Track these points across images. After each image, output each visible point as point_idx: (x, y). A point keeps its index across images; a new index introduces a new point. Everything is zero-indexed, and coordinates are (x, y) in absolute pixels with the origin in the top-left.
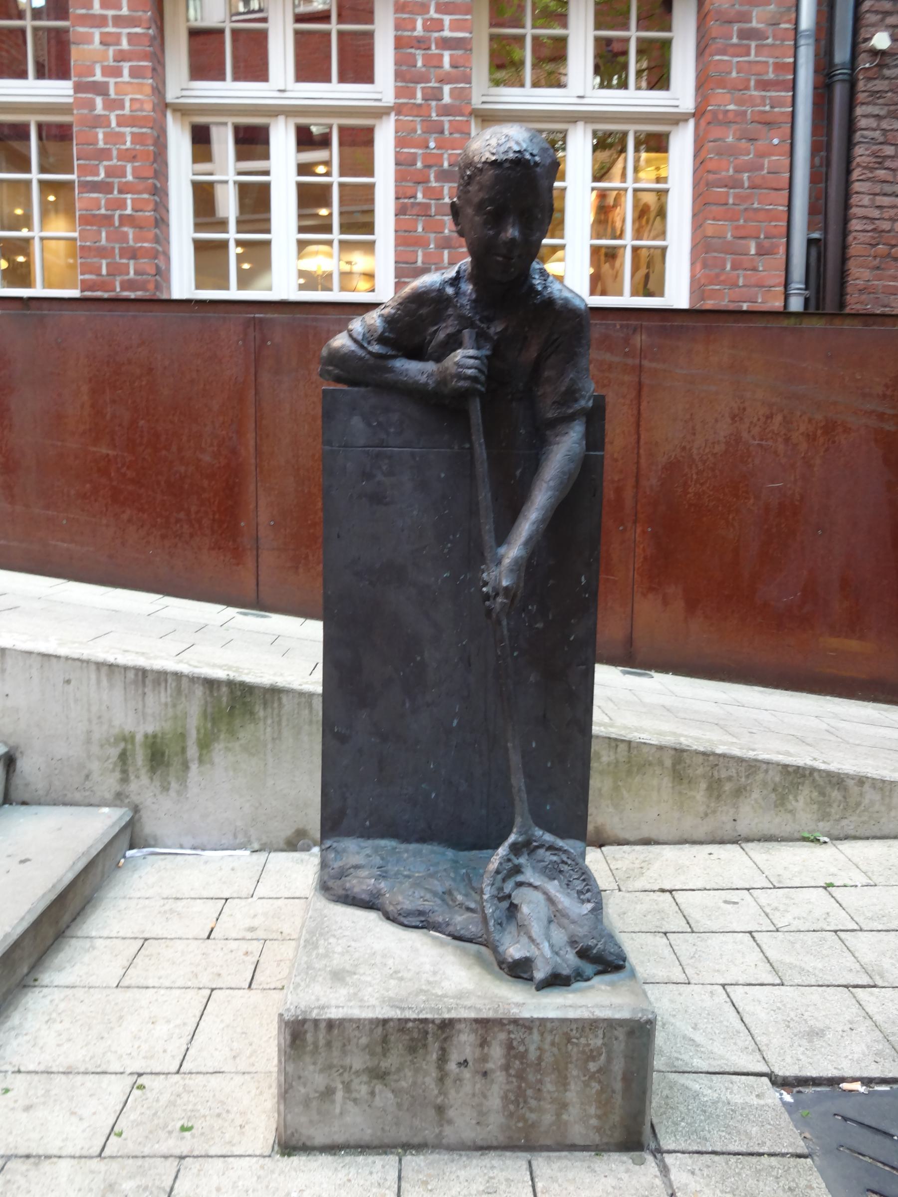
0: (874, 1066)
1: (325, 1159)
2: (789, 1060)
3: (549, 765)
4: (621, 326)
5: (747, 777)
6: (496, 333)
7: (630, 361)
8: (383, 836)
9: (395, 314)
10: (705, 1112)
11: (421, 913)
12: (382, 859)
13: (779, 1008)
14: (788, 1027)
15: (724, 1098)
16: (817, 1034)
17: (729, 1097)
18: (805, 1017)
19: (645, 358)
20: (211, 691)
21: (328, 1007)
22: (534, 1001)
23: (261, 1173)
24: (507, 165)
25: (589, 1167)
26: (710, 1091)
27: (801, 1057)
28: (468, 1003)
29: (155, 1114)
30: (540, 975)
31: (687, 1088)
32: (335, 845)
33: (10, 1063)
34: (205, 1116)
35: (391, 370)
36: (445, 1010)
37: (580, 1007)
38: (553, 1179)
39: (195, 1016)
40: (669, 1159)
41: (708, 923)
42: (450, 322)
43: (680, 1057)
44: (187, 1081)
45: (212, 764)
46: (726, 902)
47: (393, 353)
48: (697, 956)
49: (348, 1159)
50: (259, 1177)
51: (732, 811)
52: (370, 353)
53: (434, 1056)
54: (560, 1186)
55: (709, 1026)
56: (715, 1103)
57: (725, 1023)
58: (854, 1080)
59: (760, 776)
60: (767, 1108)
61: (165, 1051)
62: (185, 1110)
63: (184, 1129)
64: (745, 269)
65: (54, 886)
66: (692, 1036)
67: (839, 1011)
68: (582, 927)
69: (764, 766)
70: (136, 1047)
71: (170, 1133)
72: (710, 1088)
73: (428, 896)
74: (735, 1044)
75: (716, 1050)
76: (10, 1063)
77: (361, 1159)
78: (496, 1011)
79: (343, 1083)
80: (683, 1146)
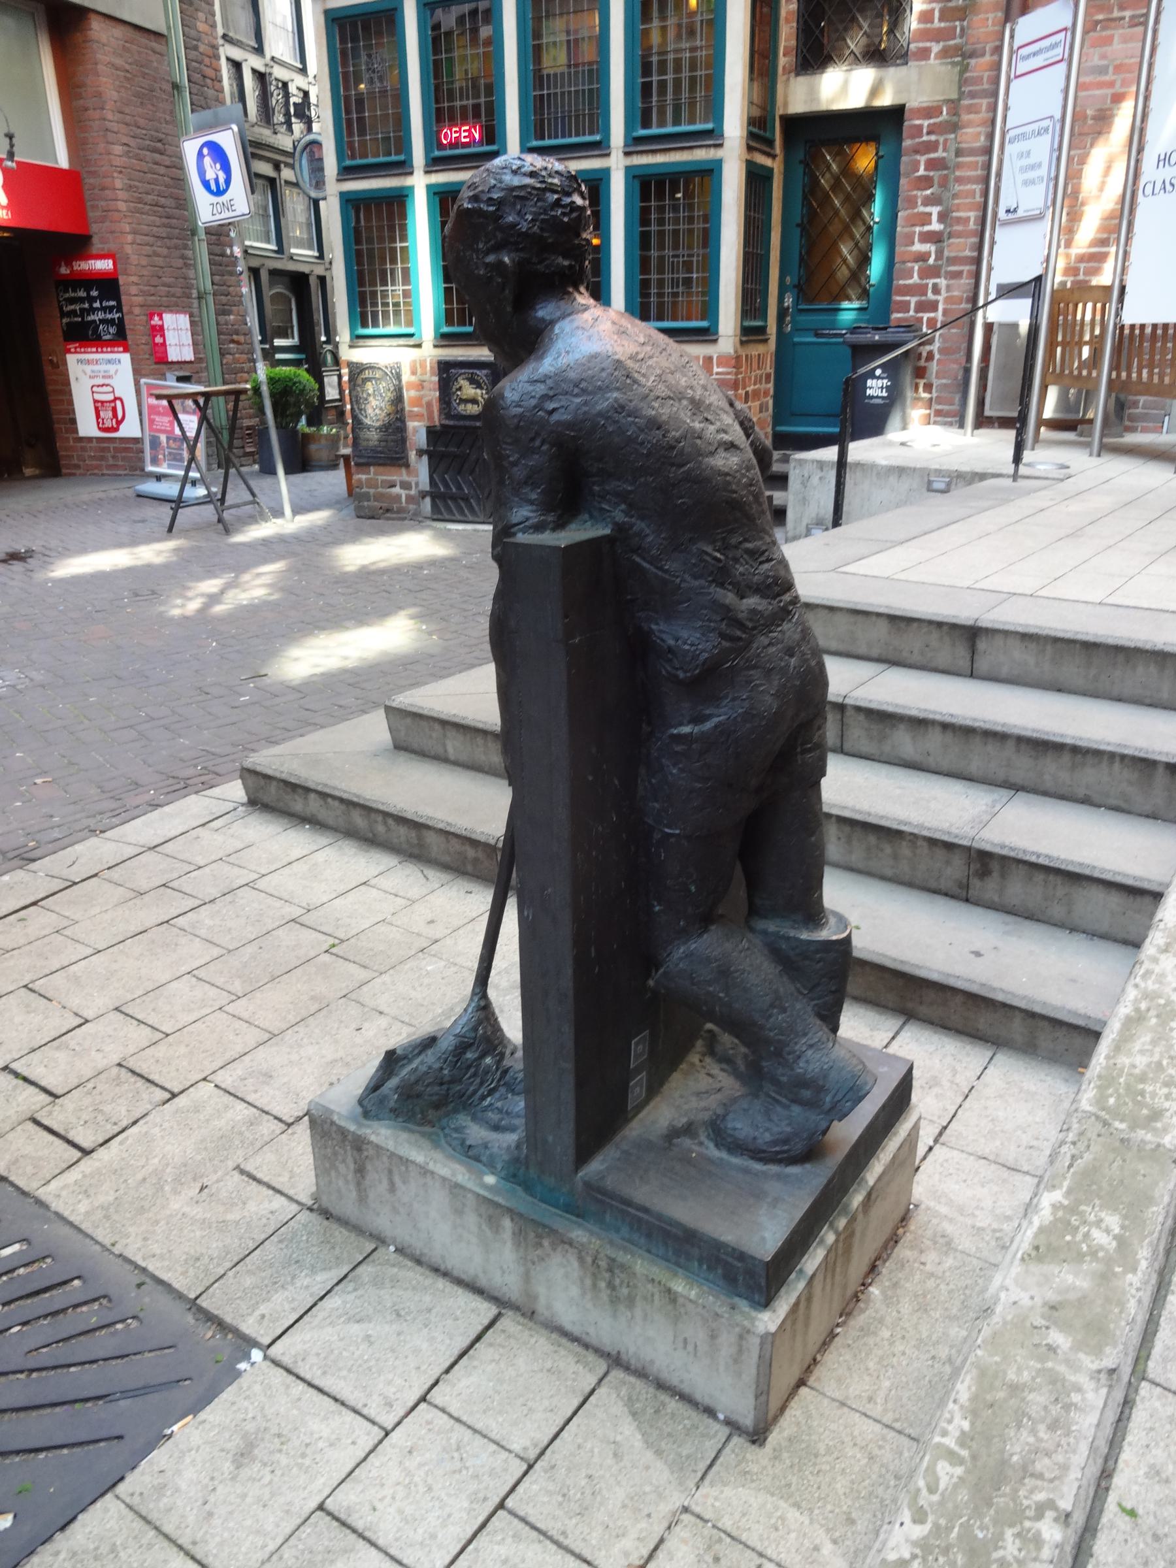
2: (257, 1388)
10: (297, 1262)
13: (303, 1456)
14: (279, 1436)
15: (290, 1288)
16: (242, 1455)
17: (286, 1293)
18: (269, 1469)
26: (305, 1283)
27: (246, 1403)
31: (325, 1269)
40: (294, 1208)
41: (503, 1551)
43: (355, 1294)
48: (456, 1455)
55: (358, 1353)
56: (294, 1277)
57: (344, 1373)
65: (902, 962)
66: (364, 1326)
67: (231, 1525)
72: (307, 1287)
74: (318, 1354)
75: (330, 1330)
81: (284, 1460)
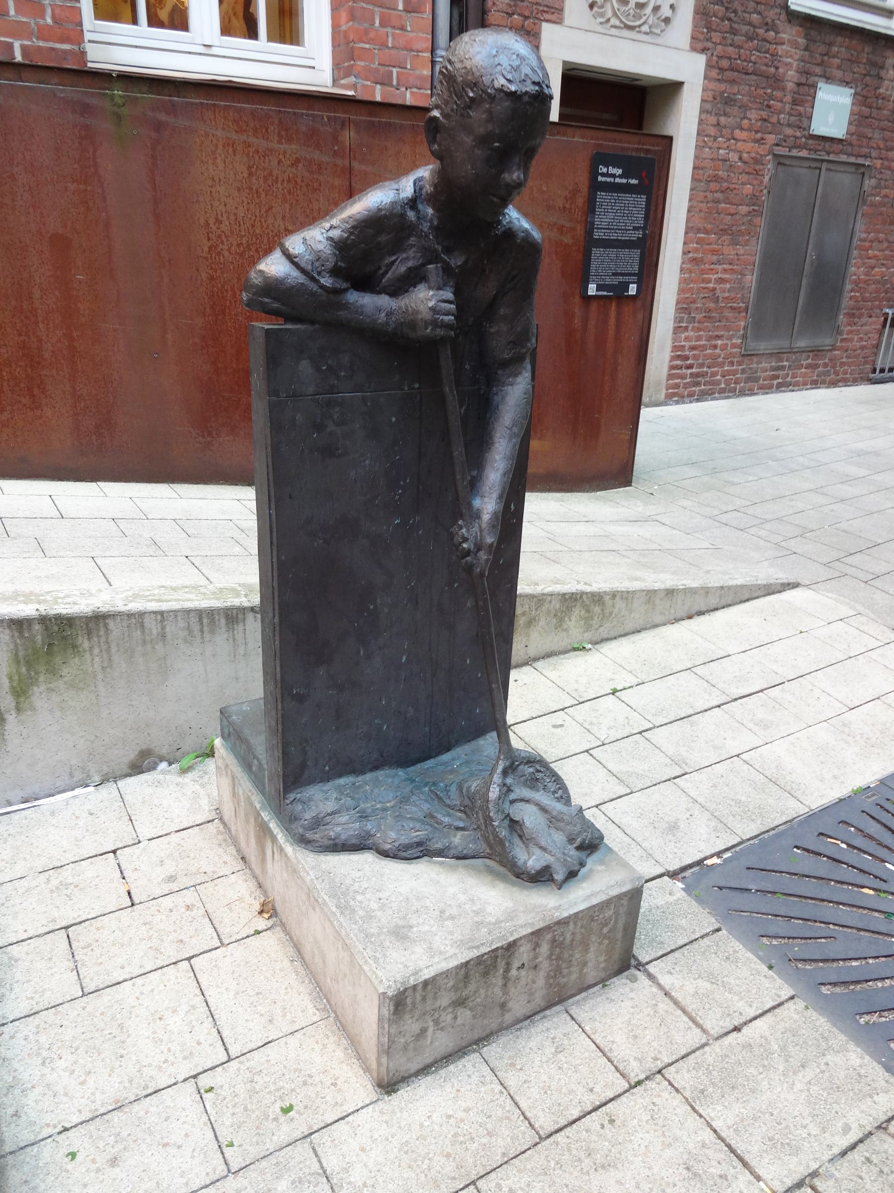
0: (718, 841)
1: (425, 1082)
2: (670, 856)
3: (479, 675)
4: (329, 118)
5: (536, 610)
6: (457, 267)
7: (339, 162)
8: (340, 776)
9: (347, 238)
11: (419, 844)
12: (353, 798)
19: (355, 159)
20: (21, 633)
21: (420, 970)
22: (565, 900)
23: (385, 1118)
24: (526, 98)
25: (607, 999)
27: (676, 850)
28: (521, 922)
29: (246, 1109)
30: (559, 877)
32: (299, 796)
33: (48, 1125)
34: (293, 1090)
35: (346, 306)
36: (508, 935)
37: (598, 892)
38: (593, 1019)
39: (196, 995)
40: (651, 968)
42: (411, 253)
44: (247, 1064)
45: (34, 709)
46: (555, 726)
47: (345, 285)
49: (443, 1072)
50: (386, 1122)
51: (524, 640)
52: (322, 287)
53: (501, 971)
54: (600, 1022)
58: (712, 856)
59: (546, 606)
60: (680, 902)
61: (199, 1043)
62: (270, 1092)
63: (286, 1110)
64: (394, 27)
68: (575, 826)
69: (549, 598)
70: (166, 1051)
71: (276, 1119)
73: (418, 825)
76: (48, 1125)
77: (452, 1067)
78: (544, 920)
79: (433, 1021)
80: (654, 955)
81: (652, 816)
